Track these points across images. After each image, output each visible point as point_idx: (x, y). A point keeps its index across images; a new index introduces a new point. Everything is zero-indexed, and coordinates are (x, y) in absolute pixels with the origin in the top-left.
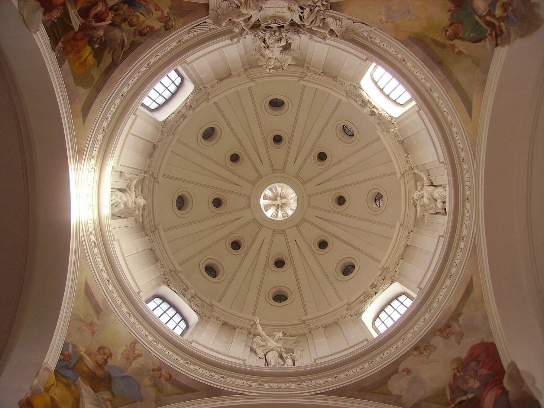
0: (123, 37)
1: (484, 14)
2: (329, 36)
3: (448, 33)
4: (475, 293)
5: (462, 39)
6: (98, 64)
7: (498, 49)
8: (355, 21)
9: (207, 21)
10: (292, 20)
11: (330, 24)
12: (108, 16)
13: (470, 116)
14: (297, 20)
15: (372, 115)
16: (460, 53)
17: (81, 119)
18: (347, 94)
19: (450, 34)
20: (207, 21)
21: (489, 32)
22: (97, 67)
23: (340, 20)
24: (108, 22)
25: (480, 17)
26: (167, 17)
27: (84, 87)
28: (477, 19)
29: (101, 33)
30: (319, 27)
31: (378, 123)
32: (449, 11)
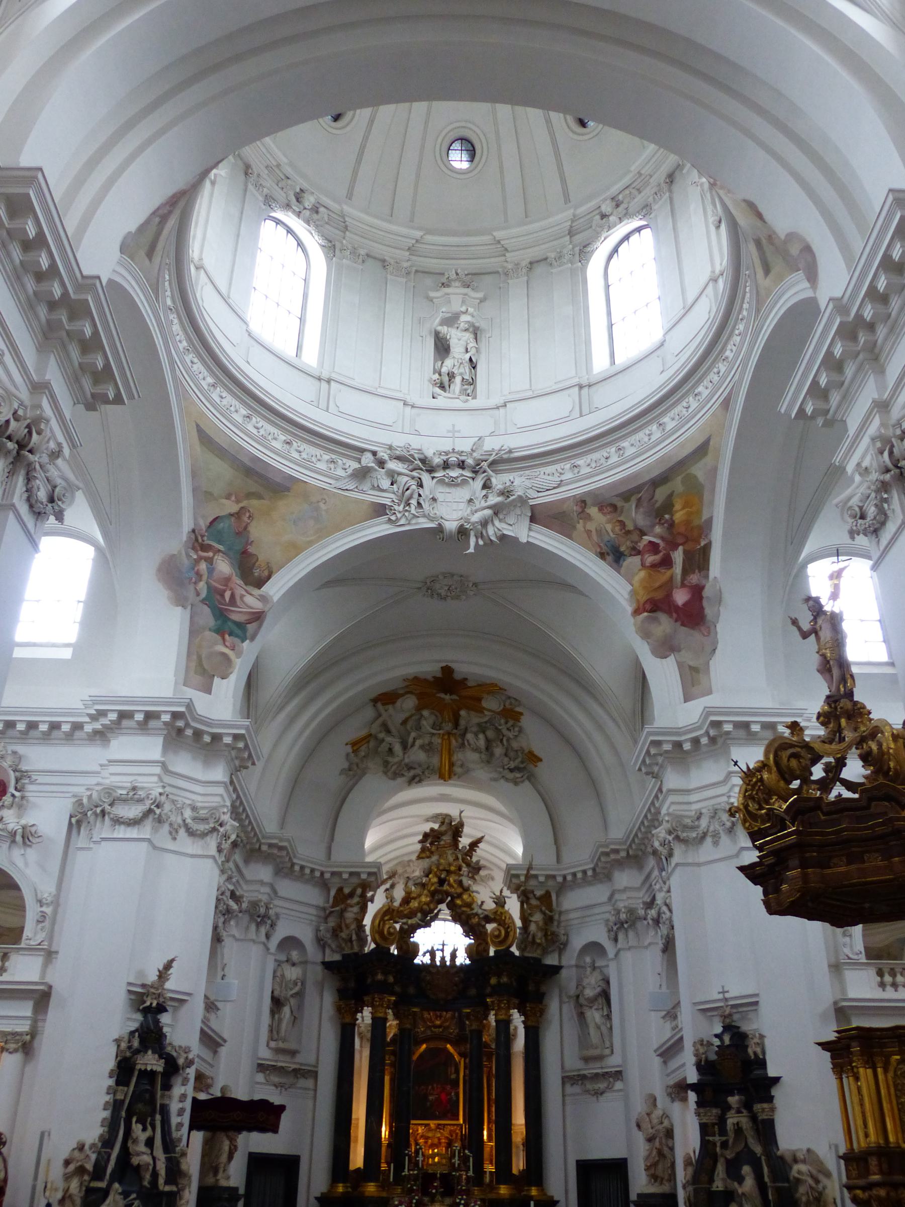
0: (636, 512)
1: (216, 557)
2: (386, 457)
3: (247, 515)
4: (142, 253)
5: (231, 515)
6: (671, 495)
7: (192, 526)
8: (356, 490)
9: (536, 495)
10: (433, 478)
11: (384, 477)
13: (198, 426)
14: (426, 477)
15: (302, 190)
16: (228, 497)
17: (711, 443)
18: (344, 219)
19: (245, 514)
20: (536, 495)
21: (205, 538)
22: (674, 491)
23: (373, 486)
24: (647, 538)
25: (219, 551)
26: (581, 519)
27: (695, 477)
28: (221, 547)
29: (658, 529)
30: (399, 474)
31: (288, 178)
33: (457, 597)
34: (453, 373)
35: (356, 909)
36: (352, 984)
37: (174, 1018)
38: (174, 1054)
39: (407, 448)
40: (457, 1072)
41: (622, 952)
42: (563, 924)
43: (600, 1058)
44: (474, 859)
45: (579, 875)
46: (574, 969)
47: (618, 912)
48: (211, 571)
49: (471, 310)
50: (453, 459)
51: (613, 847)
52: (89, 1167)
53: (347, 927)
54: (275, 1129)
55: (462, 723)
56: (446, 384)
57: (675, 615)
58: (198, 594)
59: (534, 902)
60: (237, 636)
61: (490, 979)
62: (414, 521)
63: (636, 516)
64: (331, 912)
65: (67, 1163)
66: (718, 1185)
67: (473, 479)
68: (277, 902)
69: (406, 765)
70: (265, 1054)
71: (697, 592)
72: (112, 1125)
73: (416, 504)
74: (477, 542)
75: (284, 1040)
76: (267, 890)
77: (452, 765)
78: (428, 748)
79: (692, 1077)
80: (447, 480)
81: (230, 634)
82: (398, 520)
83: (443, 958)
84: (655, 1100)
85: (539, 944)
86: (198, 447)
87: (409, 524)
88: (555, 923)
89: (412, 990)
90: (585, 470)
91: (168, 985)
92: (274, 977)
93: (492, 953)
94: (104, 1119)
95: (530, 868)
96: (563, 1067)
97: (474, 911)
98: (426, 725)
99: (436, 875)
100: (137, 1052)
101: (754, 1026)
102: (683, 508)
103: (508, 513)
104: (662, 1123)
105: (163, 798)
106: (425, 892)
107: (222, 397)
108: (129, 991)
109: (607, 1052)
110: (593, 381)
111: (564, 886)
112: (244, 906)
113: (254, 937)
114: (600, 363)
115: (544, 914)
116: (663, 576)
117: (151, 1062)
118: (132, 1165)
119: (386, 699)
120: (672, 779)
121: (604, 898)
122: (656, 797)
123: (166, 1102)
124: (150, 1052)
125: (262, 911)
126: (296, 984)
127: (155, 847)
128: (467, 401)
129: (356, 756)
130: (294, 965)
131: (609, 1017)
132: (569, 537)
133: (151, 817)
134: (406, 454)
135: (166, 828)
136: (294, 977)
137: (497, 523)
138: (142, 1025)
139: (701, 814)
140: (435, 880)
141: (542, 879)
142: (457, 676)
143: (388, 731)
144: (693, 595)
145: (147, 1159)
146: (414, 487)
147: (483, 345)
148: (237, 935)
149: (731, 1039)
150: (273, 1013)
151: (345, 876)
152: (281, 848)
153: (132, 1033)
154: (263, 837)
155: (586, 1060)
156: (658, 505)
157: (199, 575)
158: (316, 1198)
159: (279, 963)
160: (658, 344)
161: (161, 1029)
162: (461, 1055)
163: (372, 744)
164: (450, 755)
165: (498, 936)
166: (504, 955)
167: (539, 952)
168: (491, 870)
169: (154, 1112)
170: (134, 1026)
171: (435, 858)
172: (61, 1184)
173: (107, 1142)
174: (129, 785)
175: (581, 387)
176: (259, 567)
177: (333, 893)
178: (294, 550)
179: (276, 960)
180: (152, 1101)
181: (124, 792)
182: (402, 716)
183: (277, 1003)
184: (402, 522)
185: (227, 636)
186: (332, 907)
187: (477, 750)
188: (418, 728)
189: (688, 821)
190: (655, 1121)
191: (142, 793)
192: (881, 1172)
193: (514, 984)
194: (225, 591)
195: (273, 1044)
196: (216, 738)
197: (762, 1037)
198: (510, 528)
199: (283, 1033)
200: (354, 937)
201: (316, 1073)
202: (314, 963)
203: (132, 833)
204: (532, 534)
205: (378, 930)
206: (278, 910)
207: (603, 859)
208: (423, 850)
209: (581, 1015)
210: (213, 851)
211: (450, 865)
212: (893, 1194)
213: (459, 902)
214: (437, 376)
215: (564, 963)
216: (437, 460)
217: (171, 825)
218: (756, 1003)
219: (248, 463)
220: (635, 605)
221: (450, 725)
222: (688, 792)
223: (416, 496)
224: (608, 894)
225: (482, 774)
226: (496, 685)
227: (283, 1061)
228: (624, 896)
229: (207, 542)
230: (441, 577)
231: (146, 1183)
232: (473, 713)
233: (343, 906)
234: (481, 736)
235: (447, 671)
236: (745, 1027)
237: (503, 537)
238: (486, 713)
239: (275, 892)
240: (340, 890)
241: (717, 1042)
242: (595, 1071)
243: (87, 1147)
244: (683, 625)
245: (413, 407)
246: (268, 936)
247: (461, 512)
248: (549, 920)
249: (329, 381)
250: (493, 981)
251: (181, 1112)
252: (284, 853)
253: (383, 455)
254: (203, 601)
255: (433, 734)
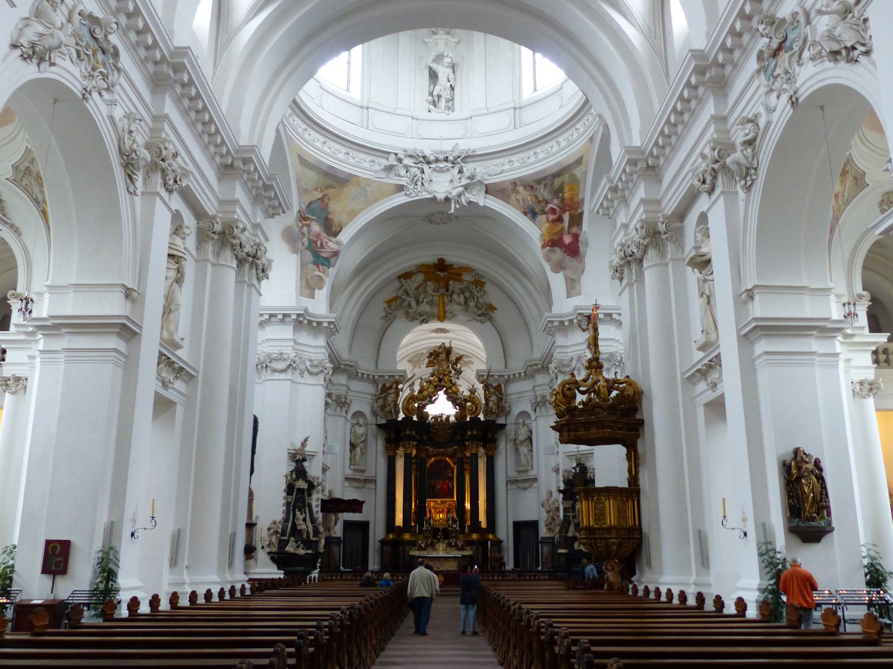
2: (402, 157)
5: (319, 199)
9: (487, 177)
10: (430, 168)
11: (402, 168)
12: (549, 209)
14: (426, 167)
16: (316, 190)
24: (550, 206)
25: (313, 220)
27: (576, 176)
28: (314, 218)
29: (556, 201)
32: (331, 213)
33: (447, 223)
34: (440, 95)
35: (393, 396)
36: (393, 436)
37: (310, 464)
38: (312, 480)
39: (415, 151)
40: (453, 473)
41: (538, 418)
42: (508, 401)
43: (526, 471)
44: (458, 367)
45: (517, 375)
46: (514, 425)
47: (536, 397)
48: (309, 231)
49: (450, 55)
50: (441, 157)
51: (534, 362)
52: (280, 531)
53: (389, 405)
54: (360, 511)
55: (451, 288)
56: (436, 101)
57: (564, 249)
58: (303, 245)
59: (492, 390)
60: (326, 265)
61: (467, 432)
62: (420, 194)
63: (544, 193)
64: (379, 398)
65: (269, 529)
66: (570, 534)
67: (453, 167)
68: (350, 393)
69: (419, 313)
70: (349, 472)
71: (576, 237)
72: (287, 513)
73: (420, 184)
74: (455, 207)
75: (358, 465)
76: (345, 388)
77: (445, 312)
78: (431, 303)
79: (562, 487)
80: (438, 169)
81: (322, 265)
82: (410, 193)
83: (442, 420)
84: (551, 493)
85: (494, 413)
86: (299, 167)
87: (417, 196)
88: (504, 401)
89: (425, 437)
90: (516, 164)
91: (307, 449)
92: (351, 432)
93: (468, 419)
94: (283, 511)
95: (489, 372)
96: (507, 476)
97: (458, 397)
98: (430, 290)
99: (437, 377)
100: (295, 480)
101: (591, 464)
102: (569, 191)
103: (473, 189)
104: (554, 504)
105: (296, 358)
106: (431, 386)
107: (310, 135)
108: (289, 453)
109: (530, 468)
110: (522, 105)
111: (508, 381)
112: (334, 398)
113: (340, 414)
114: (527, 93)
115: (498, 396)
116: (558, 227)
117: (301, 484)
118: (298, 530)
119: (407, 276)
120: (560, 340)
121: (531, 388)
122: (551, 348)
123: (310, 502)
124: (301, 480)
125: (343, 400)
126: (362, 436)
127: (293, 382)
128: (448, 114)
129: (390, 308)
130: (361, 426)
131: (531, 450)
132: (508, 203)
133: (291, 368)
134: (413, 154)
135: (298, 371)
136: (361, 432)
137: (466, 194)
138: (296, 468)
139: (572, 358)
140: (436, 379)
141: (496, 377)
142: (447, 263)
143: (408, 294)
144: (574, 239)
145: (304, 527)
146: (419, 175)
147: (458, 74)
148: (331, 414)
149: (580, 470)
150: (351, 451)
151: (387, 377)
152: (351, 366)
153: (292, 472)
154: (341, 361)
155: (519, 472)
156: (556, 188)
157: (303, 234)
158: (379, 541)
159: (353, 425)
160: (558, 88)
161: (305, 469)
162: (454, 463)
163: (399, 301)
164: (444, 307)
165: (472, 410)
166: (475, 420)
167: (494, 417)
168: (470, 357)
169: (304, 507)
170: (292, 468)
171: (436, 367)
172: (267, 538)
173: (286, 520)
174: (278, 352)
175: (515, 109)
176: (335, 226)
177: (380, 387)
178: (354, 214)
179: (351, 424)
180: (304, 502)
181: (276, 356)
182: (416, 285)
183: (353, 446)
184: (413, 195)
185: (320, 266)
186: (380, 394)
187: (459, 304)
188: (425, 291)
189: (566, 362)
190: (551, 503)
191: (285, 356)
192: (586, 535)
193: (480, 434)
194: (317, 241)
195: (352, 467)
196: (319, 323)
197: (594, 469)
198: (474, 197)
199: (357, 461)
200: (393, 411)
201: (376, 480)
202: (371, 424)
203: (282, 376)
204: (486, 200)
205: (407, 410)
206: (351, 397)
207: (529, 368)
208: (430, 362)
209: (517, 450)
210: (322, 382)
211: (445, 371)
212: (589, 541)
213: (450, 391)
214: (430, 98)
215: (508, 422)
216: (432, 158)
217: (300, 370)
218: (593, 453)
219: (327, 170)
220: (543, 243)
221: (444, 290)
222: (566, 347)
223: (420, 179)
224: (532, 386)
225: (462, 317)
226: (470, 268)
227: (358, 476)
228: (540, 389)
229: (306, 215)
230: (436, 214)
231: (305, 537)
232: (456, 282)
233: (386, 394)
234: (462, 296)
235: (441, 261)
236: (588, 464)
237: (470, 203)
238: (465, 282)
239: (349, 388)
240: (384, 385)
241: (574, 471)
242: (523, 478)
243: (277, 522)
244: (568, 255)
245: (417, 119)
246: (346, 413)
247: (446, 188)
248: (500, 399)
249: (367, 108)
250: (469, 433)
251: (317, 506)
252: (353, 368)
253: (401, 156)
254: (306, 248)
255: (434, 295)
